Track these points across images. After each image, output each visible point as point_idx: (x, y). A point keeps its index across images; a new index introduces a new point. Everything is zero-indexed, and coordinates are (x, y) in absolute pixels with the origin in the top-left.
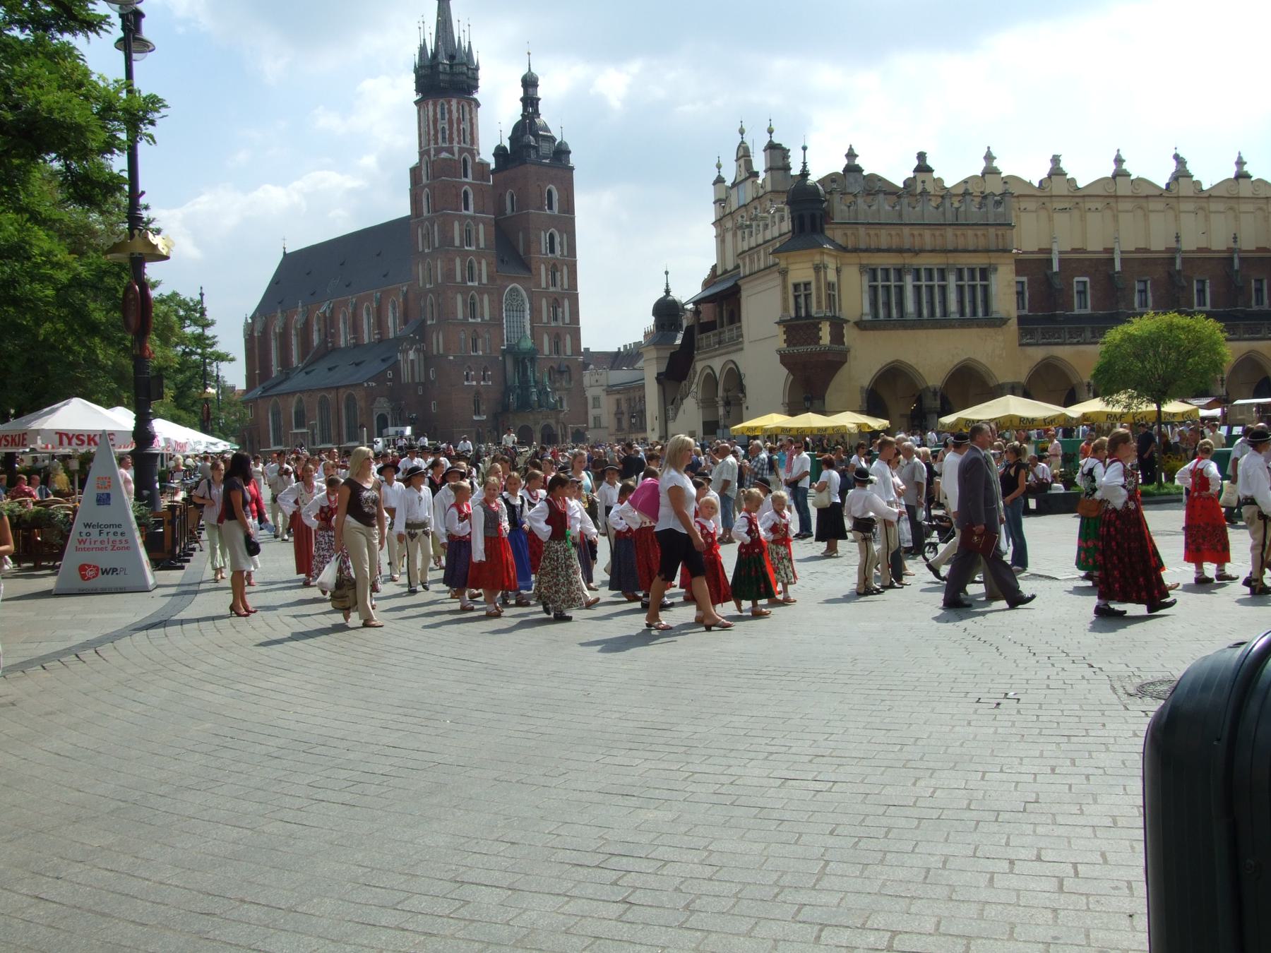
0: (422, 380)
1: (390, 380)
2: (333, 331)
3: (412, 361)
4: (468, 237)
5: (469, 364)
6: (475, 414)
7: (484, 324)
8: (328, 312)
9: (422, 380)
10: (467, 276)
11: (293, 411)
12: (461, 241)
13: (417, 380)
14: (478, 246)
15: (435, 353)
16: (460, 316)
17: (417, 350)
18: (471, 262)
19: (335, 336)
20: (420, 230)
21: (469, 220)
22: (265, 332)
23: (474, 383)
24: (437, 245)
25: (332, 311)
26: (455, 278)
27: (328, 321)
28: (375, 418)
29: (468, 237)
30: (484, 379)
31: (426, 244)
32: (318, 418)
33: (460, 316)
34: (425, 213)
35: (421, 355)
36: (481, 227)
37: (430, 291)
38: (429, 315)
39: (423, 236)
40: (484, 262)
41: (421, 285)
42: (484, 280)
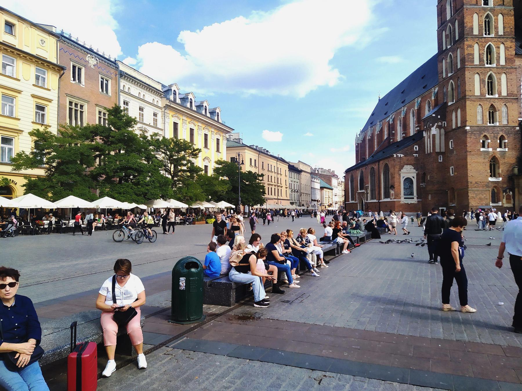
0: (443, 150)
1: (416, 152)
2: (393, 132)
3: (434, 136)
4: (488, 25)
5: (485, 134)
6: (491, 176)
7: (501, 98)
8: (391, 120)
9: (443, 150)
10: (485, 59)
11: (359, 179)
12: (480, 30)
13: (438, 150)
14: (497, 32)
15: (454, 127)
16: (477, 93)
17: (439, 127)
18: (489, 47)
19: (394, 135)
20: (444, 32)
21: (488, 12)
22: (364, 140)
23: (490, 150)
24: (457, 38)
25: (393, 120)
26: (473, 61)
27: (391, 126)
28: (402, 181)
29: (488, 25)
30: (500, 147)
31: (448, 43)
32: (369, 183)
33: (477, 93)
34: (448, 17)
35: (443, 131)
36: (500, 17)
37: (451, 78)
38: (450, 98)
39: (446, 35)
40: (502, 47)
41: (444, 76)
42: (502, 62)
